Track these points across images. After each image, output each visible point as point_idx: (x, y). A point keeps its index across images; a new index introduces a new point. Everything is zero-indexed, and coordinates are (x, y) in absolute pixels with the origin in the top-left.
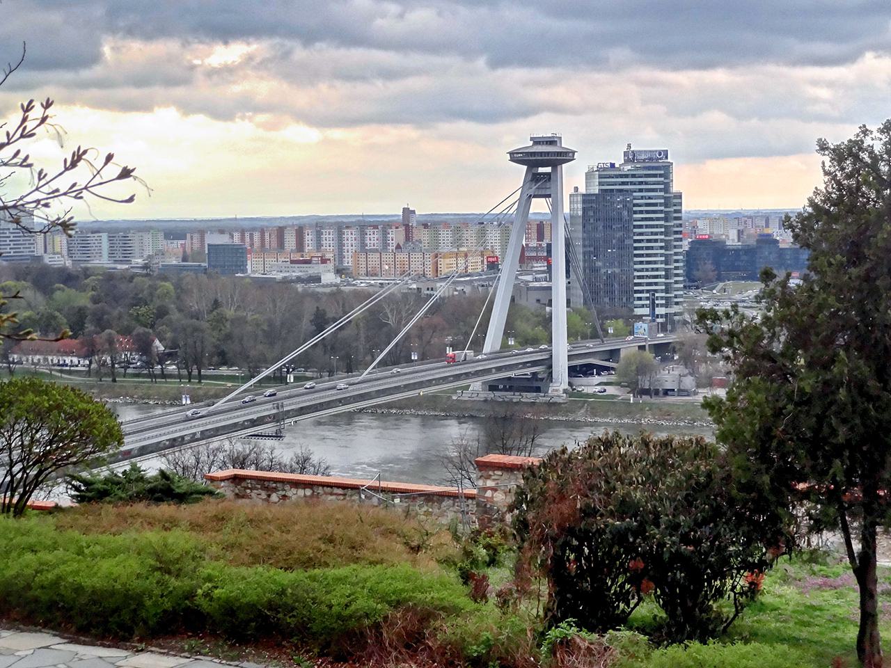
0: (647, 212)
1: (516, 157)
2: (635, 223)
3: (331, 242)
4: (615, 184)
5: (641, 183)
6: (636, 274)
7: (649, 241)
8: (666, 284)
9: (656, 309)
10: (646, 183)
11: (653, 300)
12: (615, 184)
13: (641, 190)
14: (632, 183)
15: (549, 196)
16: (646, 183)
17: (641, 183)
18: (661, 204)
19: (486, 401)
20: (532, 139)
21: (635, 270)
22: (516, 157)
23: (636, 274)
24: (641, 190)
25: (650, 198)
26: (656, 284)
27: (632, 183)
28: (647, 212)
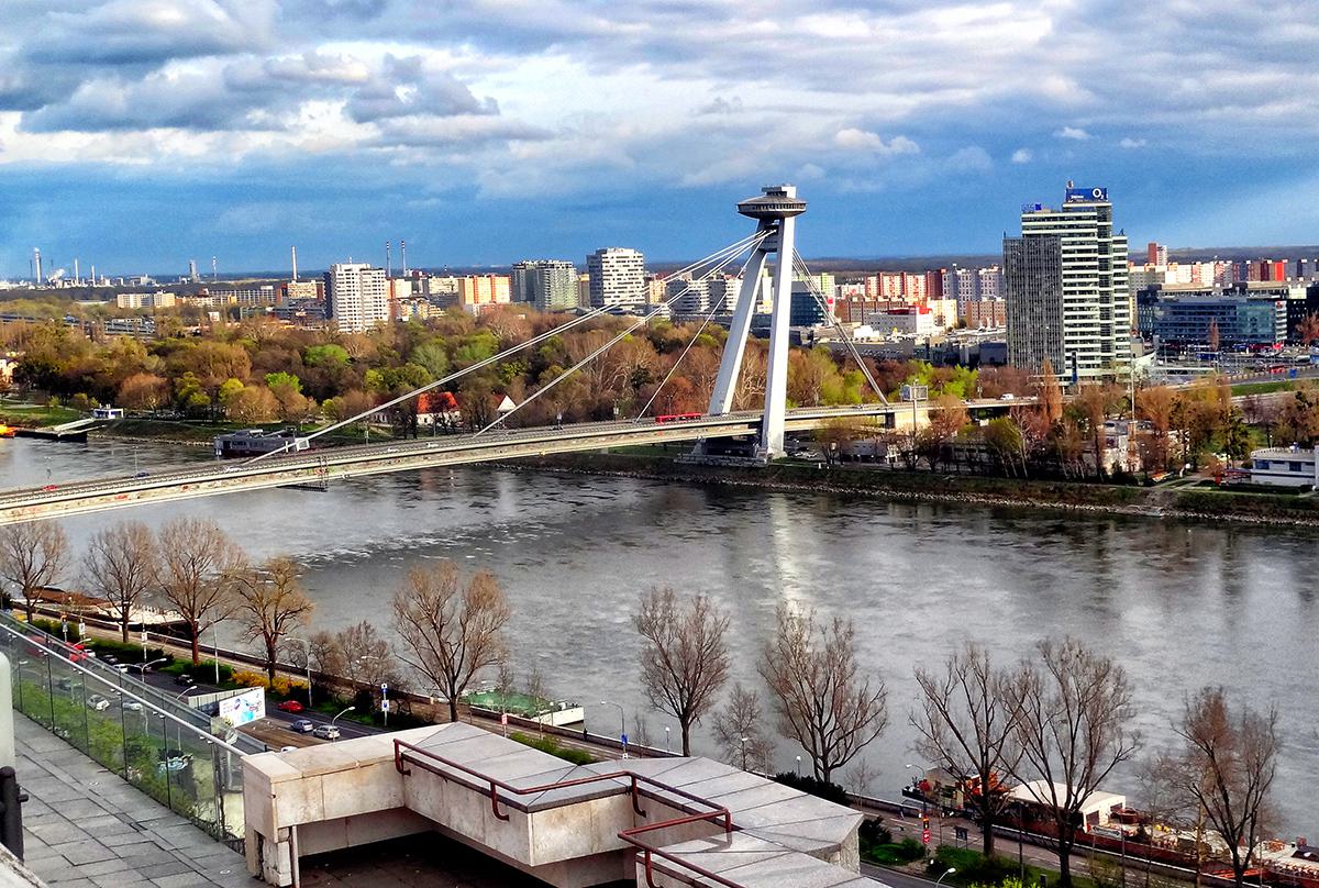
0: (1081, 259)
1: (748, 210)
2: (1065, 272)
3: (969, 288)
4: (1040, 228)
5: (1070, 227)
6: (1067, 329)
7: (1082, 292)
8: (1103, 342)
9: (1078, 370)
10: (1078, 227)
11: (1074, 363)
12: (1040, 228)
13: (1071, 235)
14: (1061, 227)
15: (775, 250)
16: (1078, 227)
17: (1070, 227)
18: (1095, 251)
19: (700, 465)
20: (764, 190)
21: (1066, 325)
22: (748, 210)
23: (1067, 329)
24: (1071, 235)
25: (1081, 244)
26: (1091, 341)
27: (1061, 227)
28: (1081, 259)
